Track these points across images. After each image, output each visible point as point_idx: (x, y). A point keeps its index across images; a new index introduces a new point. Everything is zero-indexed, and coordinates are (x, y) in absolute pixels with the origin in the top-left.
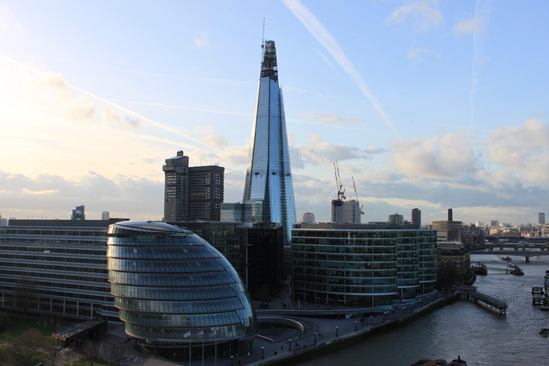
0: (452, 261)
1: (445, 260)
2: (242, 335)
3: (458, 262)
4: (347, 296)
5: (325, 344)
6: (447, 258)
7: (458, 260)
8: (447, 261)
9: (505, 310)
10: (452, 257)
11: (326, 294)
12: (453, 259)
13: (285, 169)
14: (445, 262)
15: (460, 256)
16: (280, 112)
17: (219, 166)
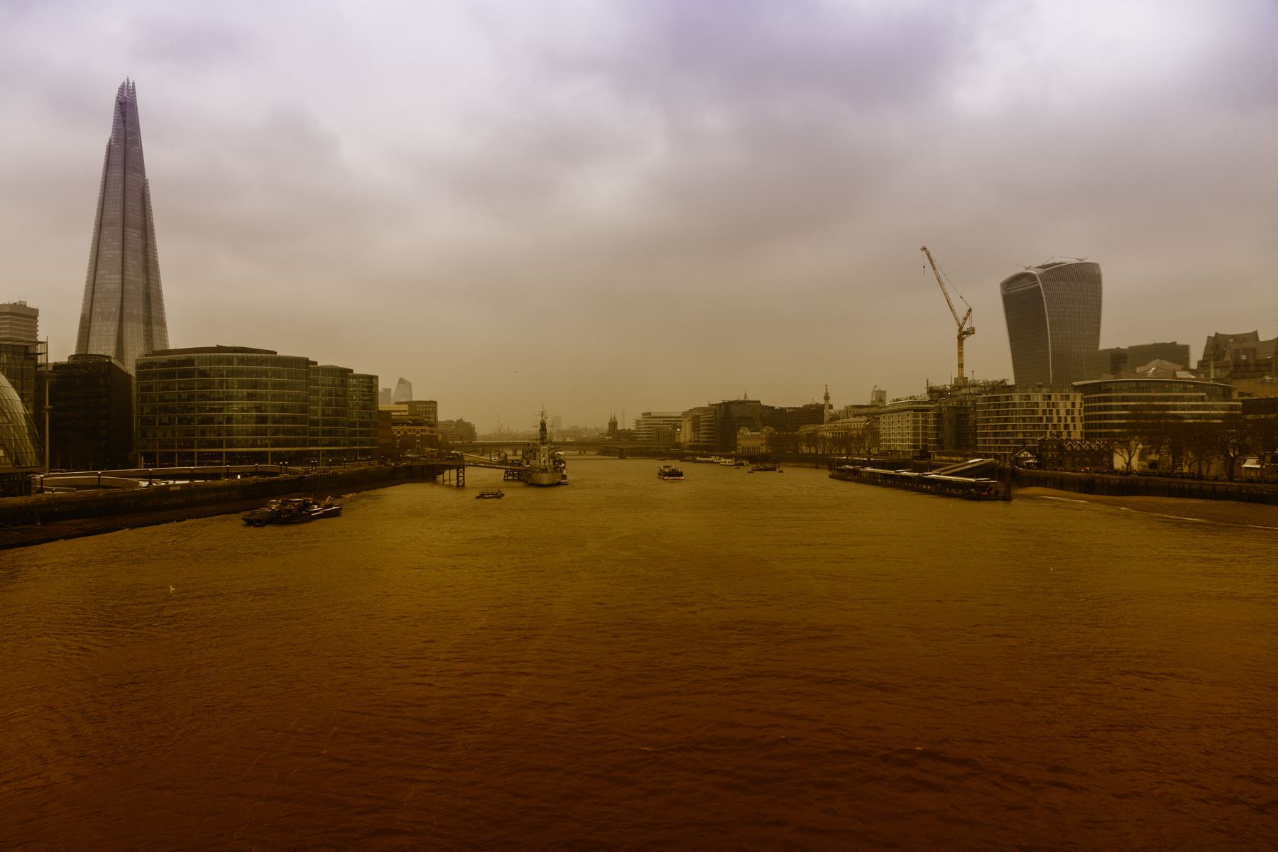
0: (408, 433)
1: (399, 432)
2: (6, 464)
3: (418, 435)
4: (226, 452)
5: (169, 489)
6: (402, 430)
7: (418, 433)
8: (402, 433)
9: (464, 470)
10: (409, 428)
11: (193, 453)
12: (410, 430)
13: (154, 314)
14: (398, 435)
15: (420, 428)
16: (145, 221)
17: (28, 305)
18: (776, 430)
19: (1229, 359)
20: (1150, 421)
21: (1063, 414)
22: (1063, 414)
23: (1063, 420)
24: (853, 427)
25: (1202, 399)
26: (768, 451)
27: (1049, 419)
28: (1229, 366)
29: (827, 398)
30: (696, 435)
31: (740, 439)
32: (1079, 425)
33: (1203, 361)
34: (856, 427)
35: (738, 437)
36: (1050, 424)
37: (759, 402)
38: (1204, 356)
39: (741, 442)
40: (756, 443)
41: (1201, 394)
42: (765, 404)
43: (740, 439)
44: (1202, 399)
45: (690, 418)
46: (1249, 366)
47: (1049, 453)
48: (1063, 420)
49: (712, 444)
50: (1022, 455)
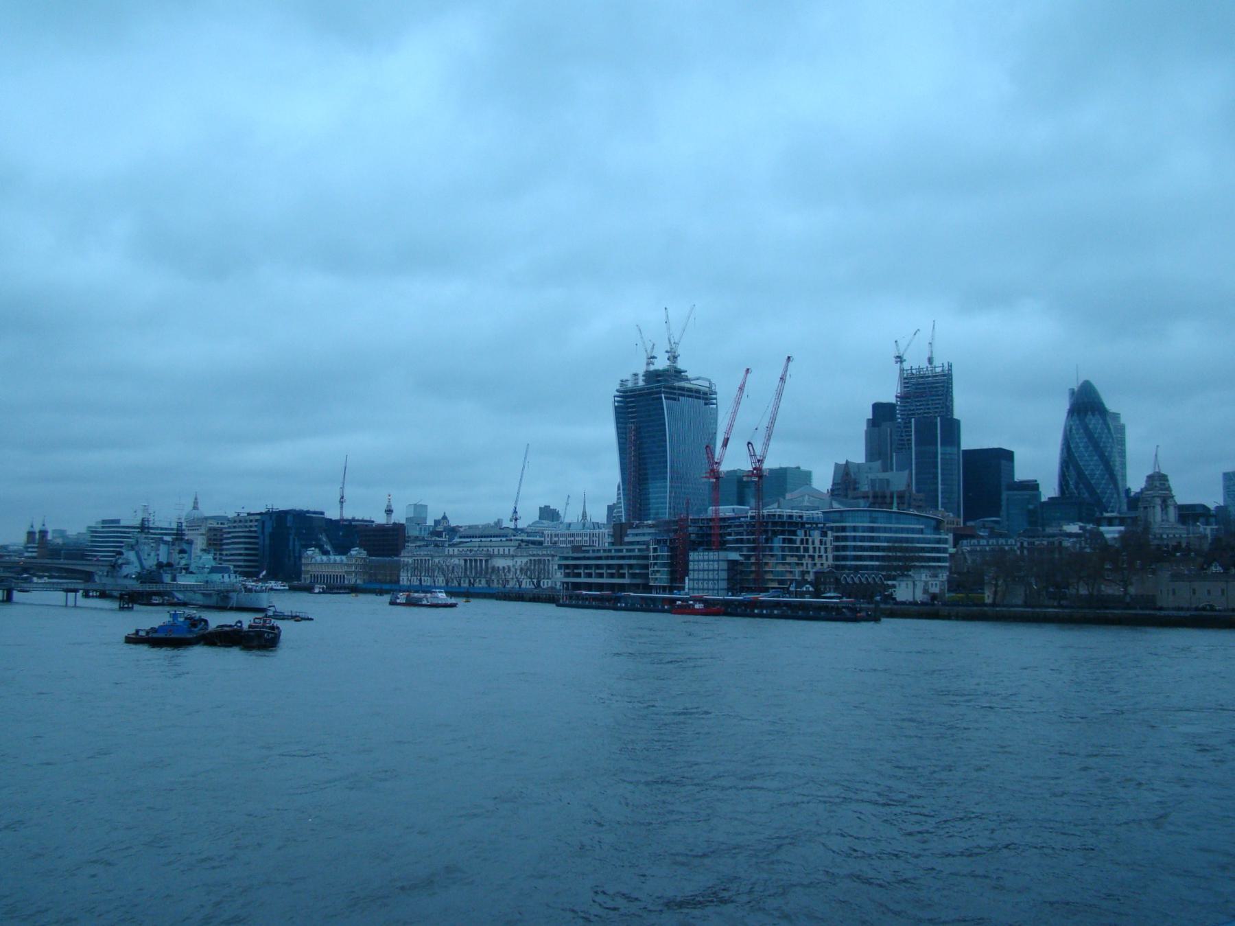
18: (370, 555)
19: (867, 490)
20: (899, 554)
21: (817, 544)
22: (817, 544)
23: (817, 550)
24: (496, 552)
25: (921, 531)
26: (358, 582)
27: (806, 550)
28: (868, 497)
29: (389, 511)
30: (218, 557)
31: (306, 564)
32: (830, 556)
33: (832, 490)
34: (501, 552)
35: (303, 561)
36: (806, 554)
37: (322, 513)
38: (834, 484)
39: (309, 568)
40: (339, 571)
41: (918, 526)
42: (328, 517)
43: (307, 565)
44: (921, 531)
45: (203, 531)
46: (885, 497)
47: (827, 586)
48: (817, 550)
49: (253, 570)
50: (804, 589)
